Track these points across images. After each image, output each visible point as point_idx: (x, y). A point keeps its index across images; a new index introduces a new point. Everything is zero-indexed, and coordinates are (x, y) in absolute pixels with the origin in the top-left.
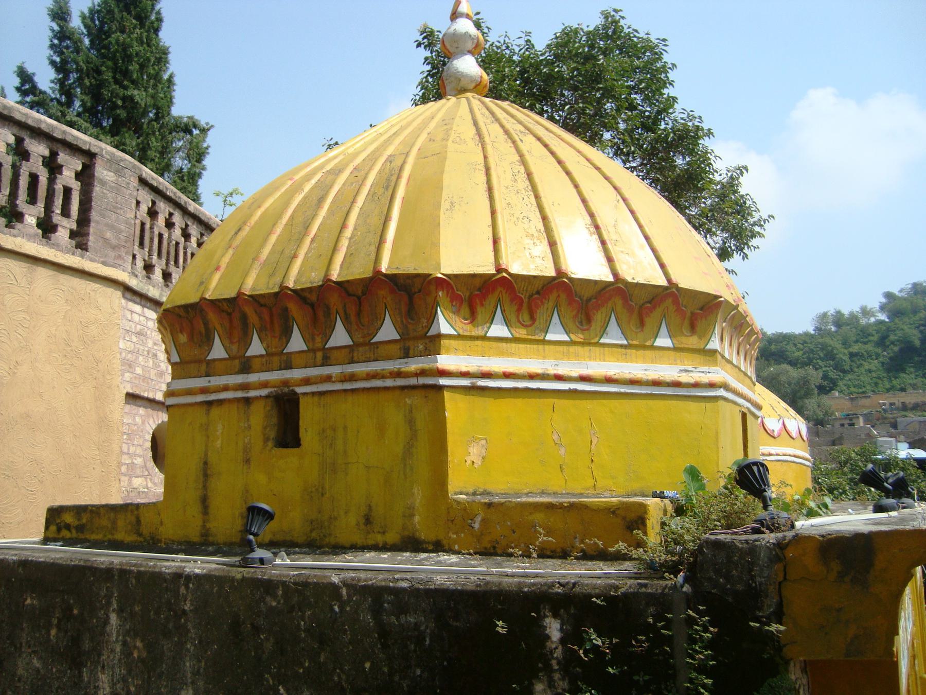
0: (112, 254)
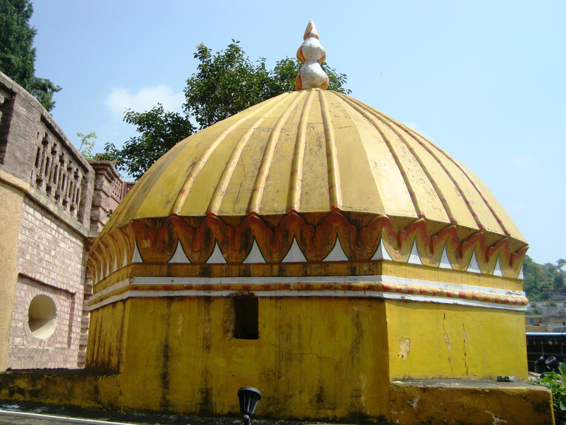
0: (19, 169)
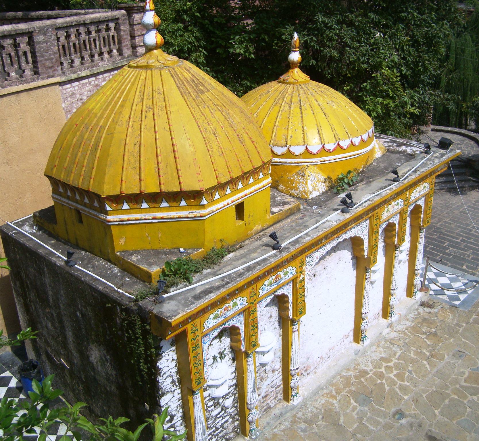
0: (51, 71)
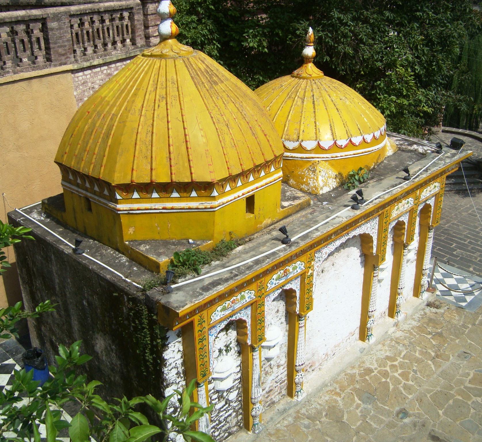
0: (63, 58)
